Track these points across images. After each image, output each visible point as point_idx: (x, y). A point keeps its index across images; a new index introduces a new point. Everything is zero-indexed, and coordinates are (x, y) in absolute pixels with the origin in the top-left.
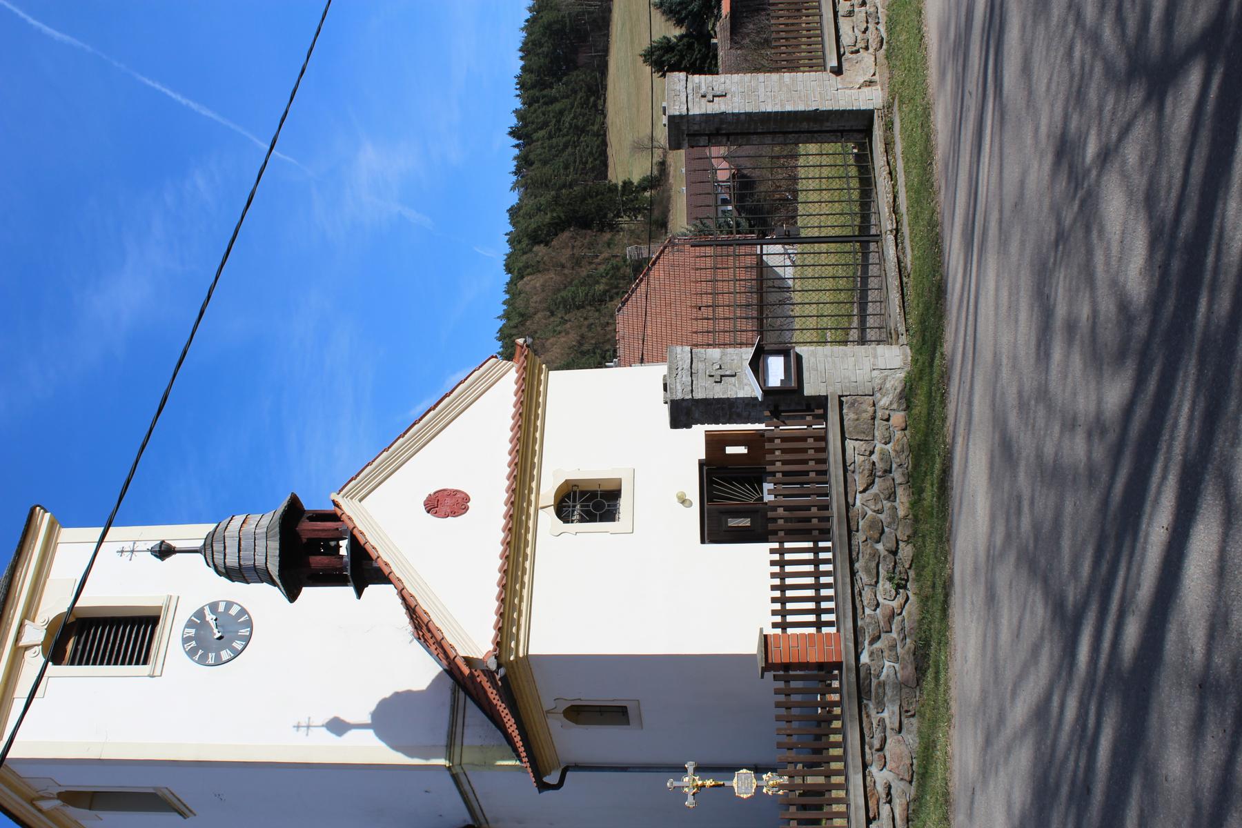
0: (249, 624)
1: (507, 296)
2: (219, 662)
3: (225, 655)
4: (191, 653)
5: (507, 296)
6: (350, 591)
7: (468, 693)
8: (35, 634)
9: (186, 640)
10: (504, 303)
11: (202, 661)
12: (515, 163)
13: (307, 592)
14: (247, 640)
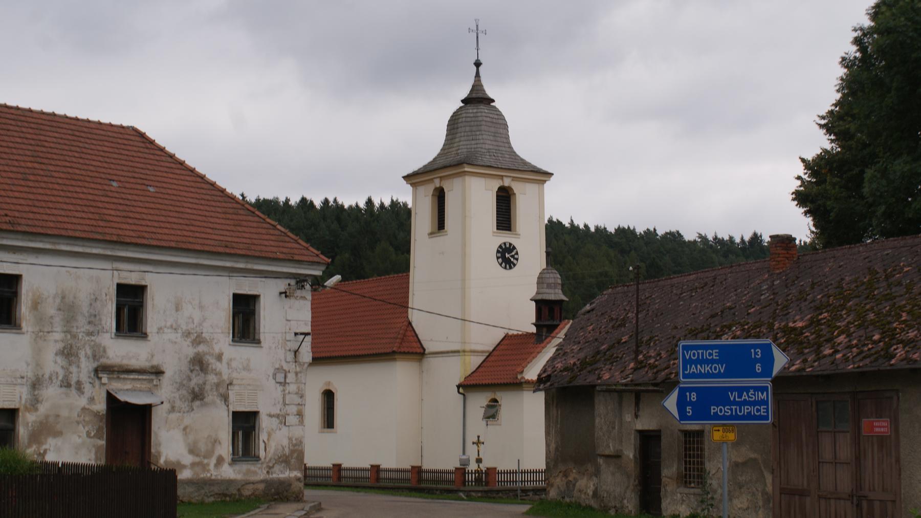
0: (511, 268)
1: (593, 229)
2: (498, 258)
3: (500, 260)
4: (500, 247)
5: (593, 229)
6: (534, 321)
7: (488, 357)
8: (507, 182)
9: (505, 244)
10: (586, 226)
11: (498, 252)
12: (726, 238)
13: (534, 303)
14: (505, 268)
